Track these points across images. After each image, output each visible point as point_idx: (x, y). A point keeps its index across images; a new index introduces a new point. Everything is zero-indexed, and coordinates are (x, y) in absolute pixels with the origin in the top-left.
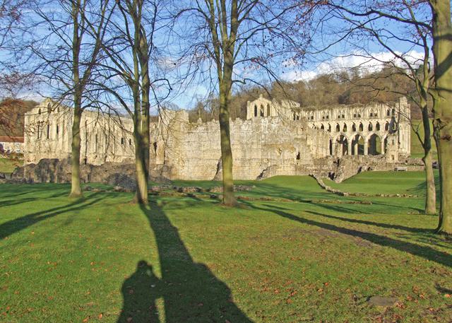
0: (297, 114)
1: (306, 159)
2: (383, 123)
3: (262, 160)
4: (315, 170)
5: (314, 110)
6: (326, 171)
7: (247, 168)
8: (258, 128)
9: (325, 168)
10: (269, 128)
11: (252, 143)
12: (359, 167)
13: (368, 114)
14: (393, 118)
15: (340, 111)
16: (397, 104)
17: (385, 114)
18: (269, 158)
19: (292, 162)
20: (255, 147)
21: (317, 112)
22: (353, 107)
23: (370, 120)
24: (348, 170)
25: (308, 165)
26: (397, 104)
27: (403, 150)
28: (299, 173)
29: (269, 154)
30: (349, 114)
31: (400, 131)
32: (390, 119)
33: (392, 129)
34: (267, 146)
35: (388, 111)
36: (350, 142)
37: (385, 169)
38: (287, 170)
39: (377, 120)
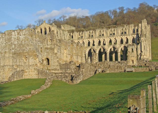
0: (71, 34)
1: (54, 63)
2: (130, 38)
3: (13, 66)
4: (61, 73)
5: (83, 31)
6: (69, 73)
7: (2, 73)
8: (10, 40)
9: (69, 71)
10: (18, 39)
11: (5, 52)
12: (95, 69)
13: (120, 32)
14: (138, 34)
15: (100, 31)
16: (140, 25)
17: (131, 32)
18: (18, 64)
19: (36, 67)
20: (7, 55)
21: (85, 32)
22: (109, 28)
23: (121, 37)
24: (87, 73)
25: (56, 69)
26: (140, 25)
27: (145, 57)
28: (40, 77)
29: (18, 61)
30: (107, 33)
31: (142, 43)
32: (135, 35)
33: (137, 41)
34: (17, 54)
35: (134, 30)
36: (108, 52)
37: (117, 71)
38: (31, 74)
39: (126, 36)
